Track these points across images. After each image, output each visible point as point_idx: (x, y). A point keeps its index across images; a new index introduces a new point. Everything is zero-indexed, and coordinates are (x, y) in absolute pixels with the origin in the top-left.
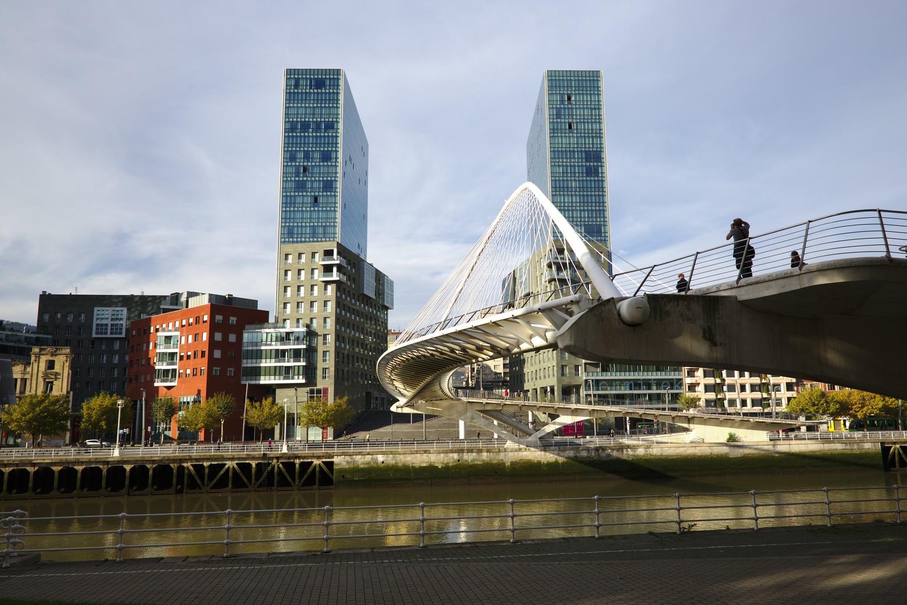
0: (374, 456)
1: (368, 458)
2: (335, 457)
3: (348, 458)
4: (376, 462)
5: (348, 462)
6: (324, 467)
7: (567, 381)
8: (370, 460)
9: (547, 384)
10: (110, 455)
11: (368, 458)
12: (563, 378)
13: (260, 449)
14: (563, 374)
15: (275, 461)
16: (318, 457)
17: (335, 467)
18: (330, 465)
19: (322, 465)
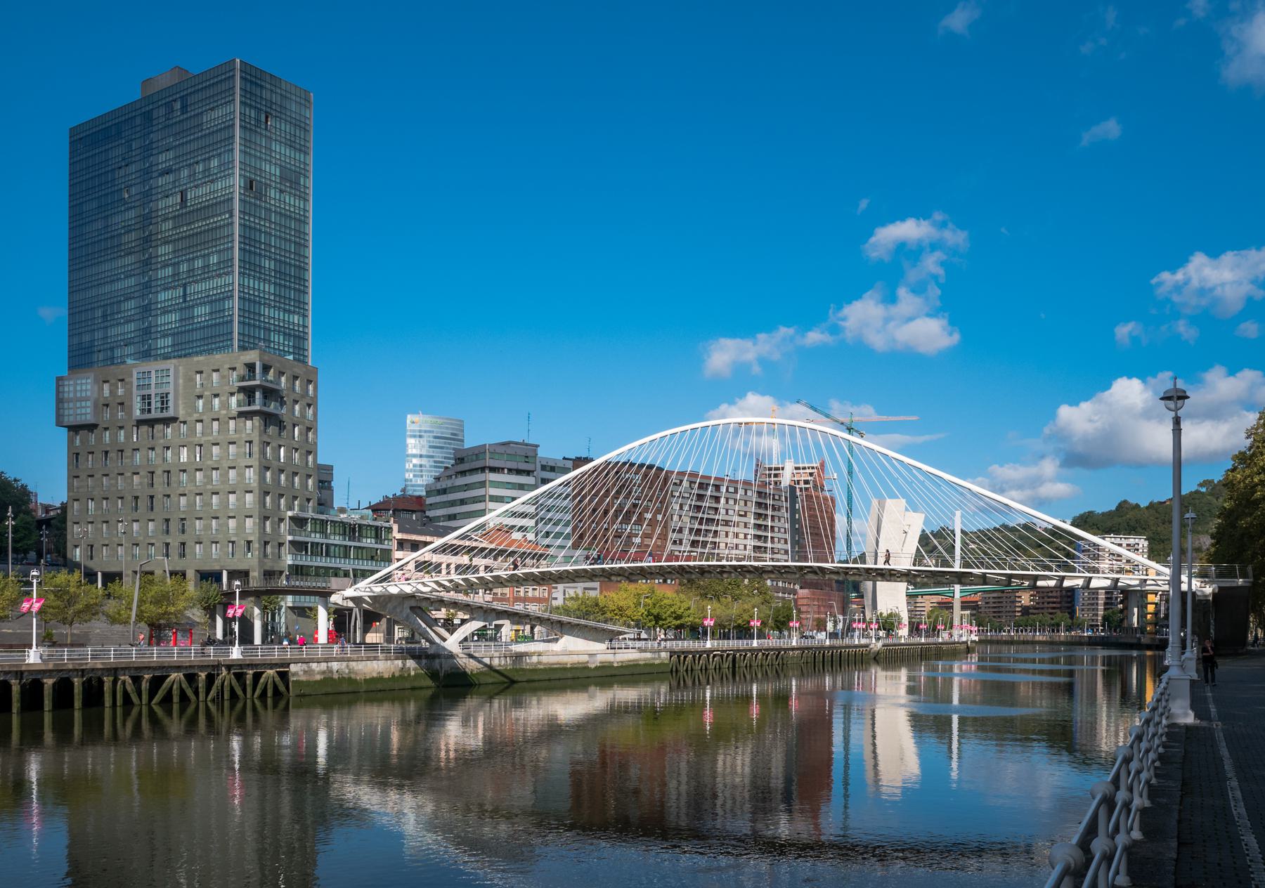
0: (330, 664)
1: (323, 666)
2: (292, 666)
3: (305, 666)
4: (331, 672)
5: (305, 672)
6: (277, 679)
7: (269, 565)
8: (325, 668)
9: (221, 566)
10: (25, 660)
11: (323, 666)
12: (266, 560)
13: (62, 655)
14: (265, 555)
15: (224, 672)
16: (272, 666)
17: (292, 679)
18: (284, 676)
19: (276, 675)
